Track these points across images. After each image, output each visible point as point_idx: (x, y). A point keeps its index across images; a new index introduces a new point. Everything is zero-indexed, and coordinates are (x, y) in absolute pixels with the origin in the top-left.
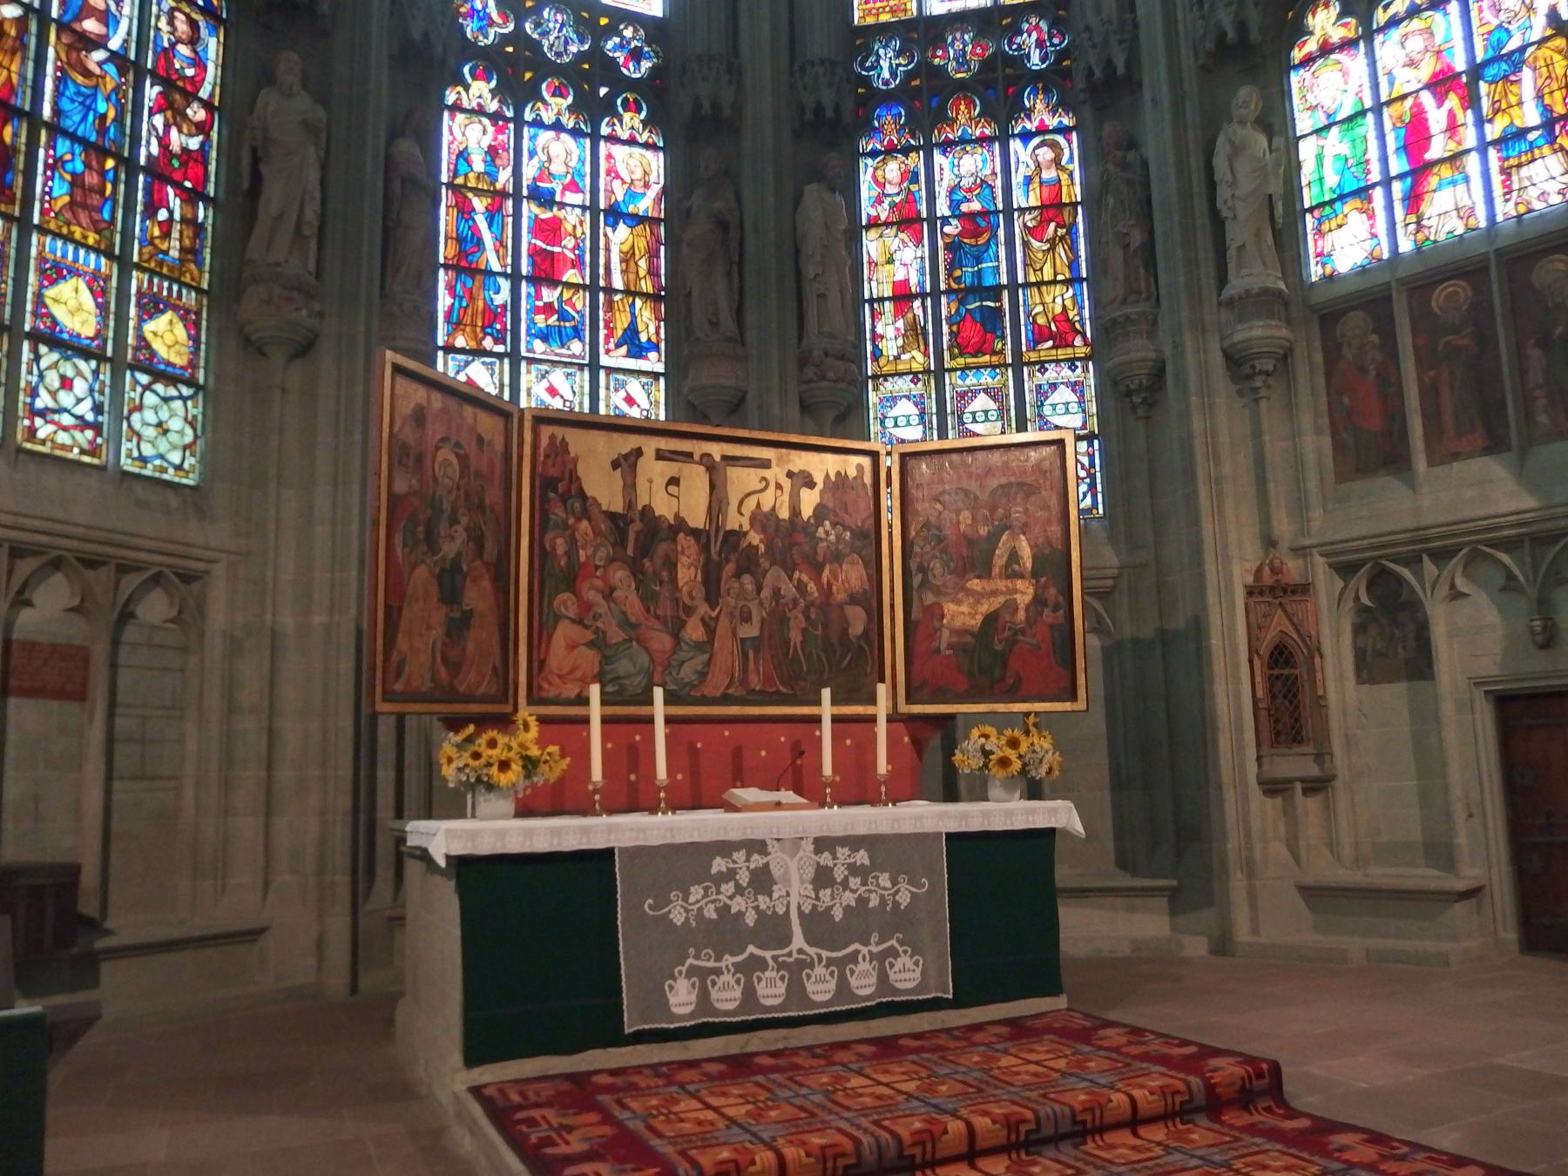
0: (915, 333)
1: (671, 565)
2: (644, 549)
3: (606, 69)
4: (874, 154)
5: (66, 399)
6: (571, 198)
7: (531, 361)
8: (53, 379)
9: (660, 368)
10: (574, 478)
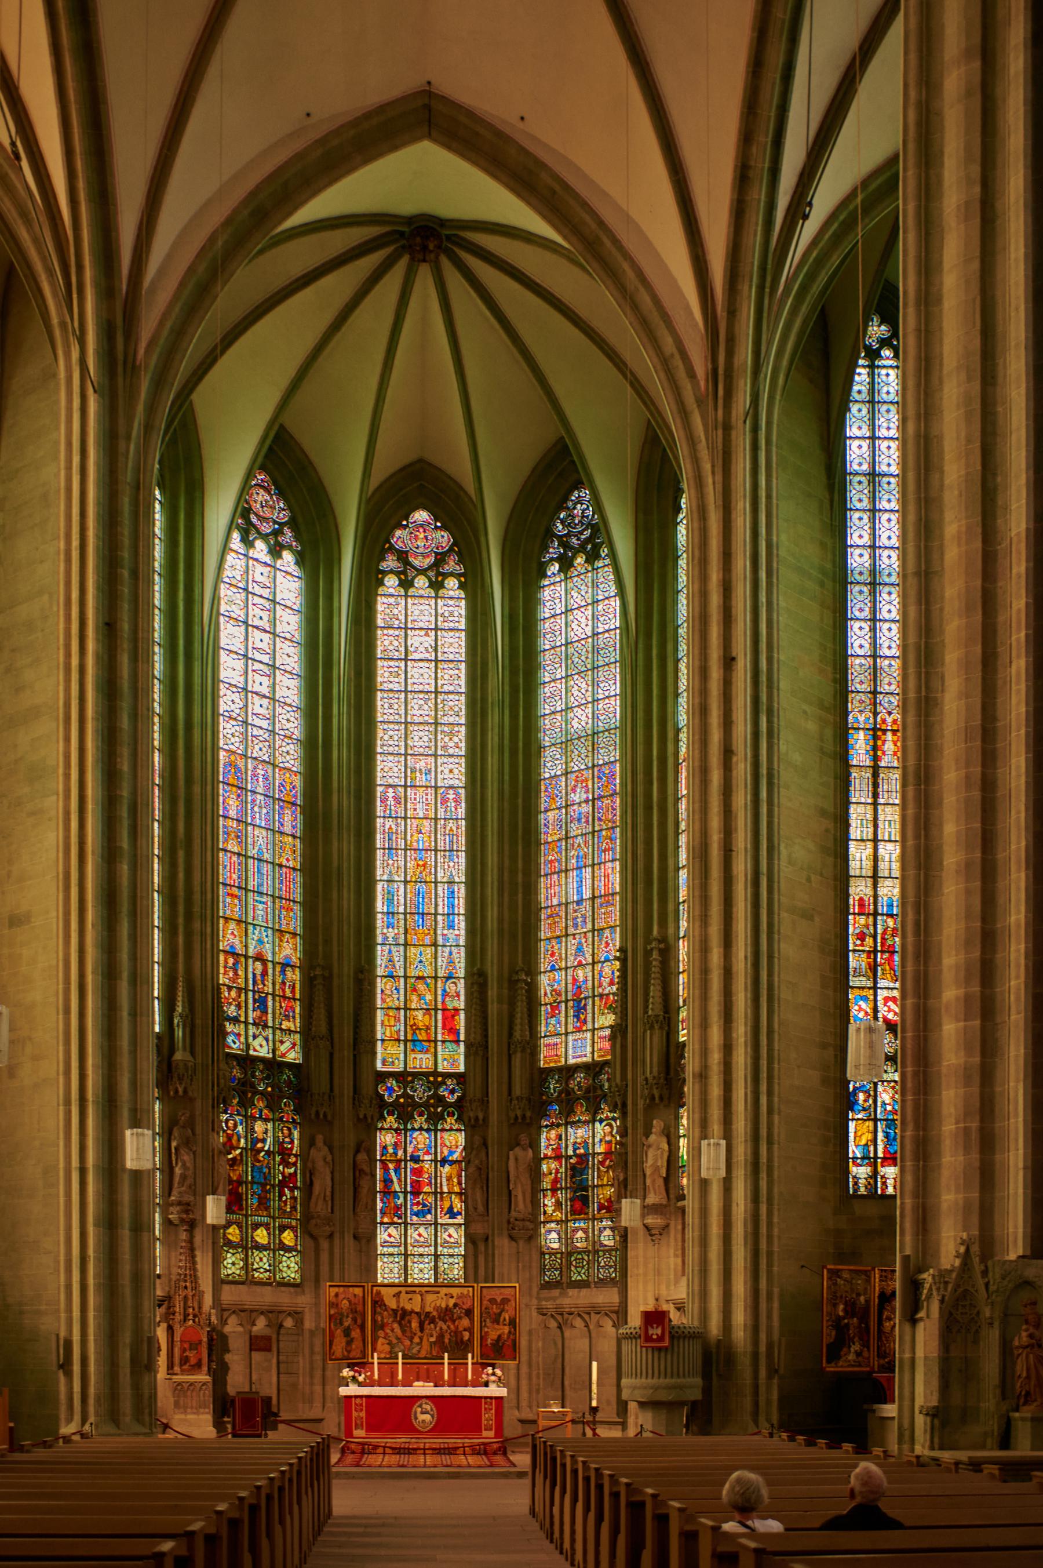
0: (558, 1205)
1: (410, 1322)
2: (403, 1318)
3: (441, 1100)
4: (546, 1126)
5: (261, 1264)
6: (426, 1158)
7: (412, 1224)
8: (257, 1259)
9: (462, 1221)
10: (383, 1300)
